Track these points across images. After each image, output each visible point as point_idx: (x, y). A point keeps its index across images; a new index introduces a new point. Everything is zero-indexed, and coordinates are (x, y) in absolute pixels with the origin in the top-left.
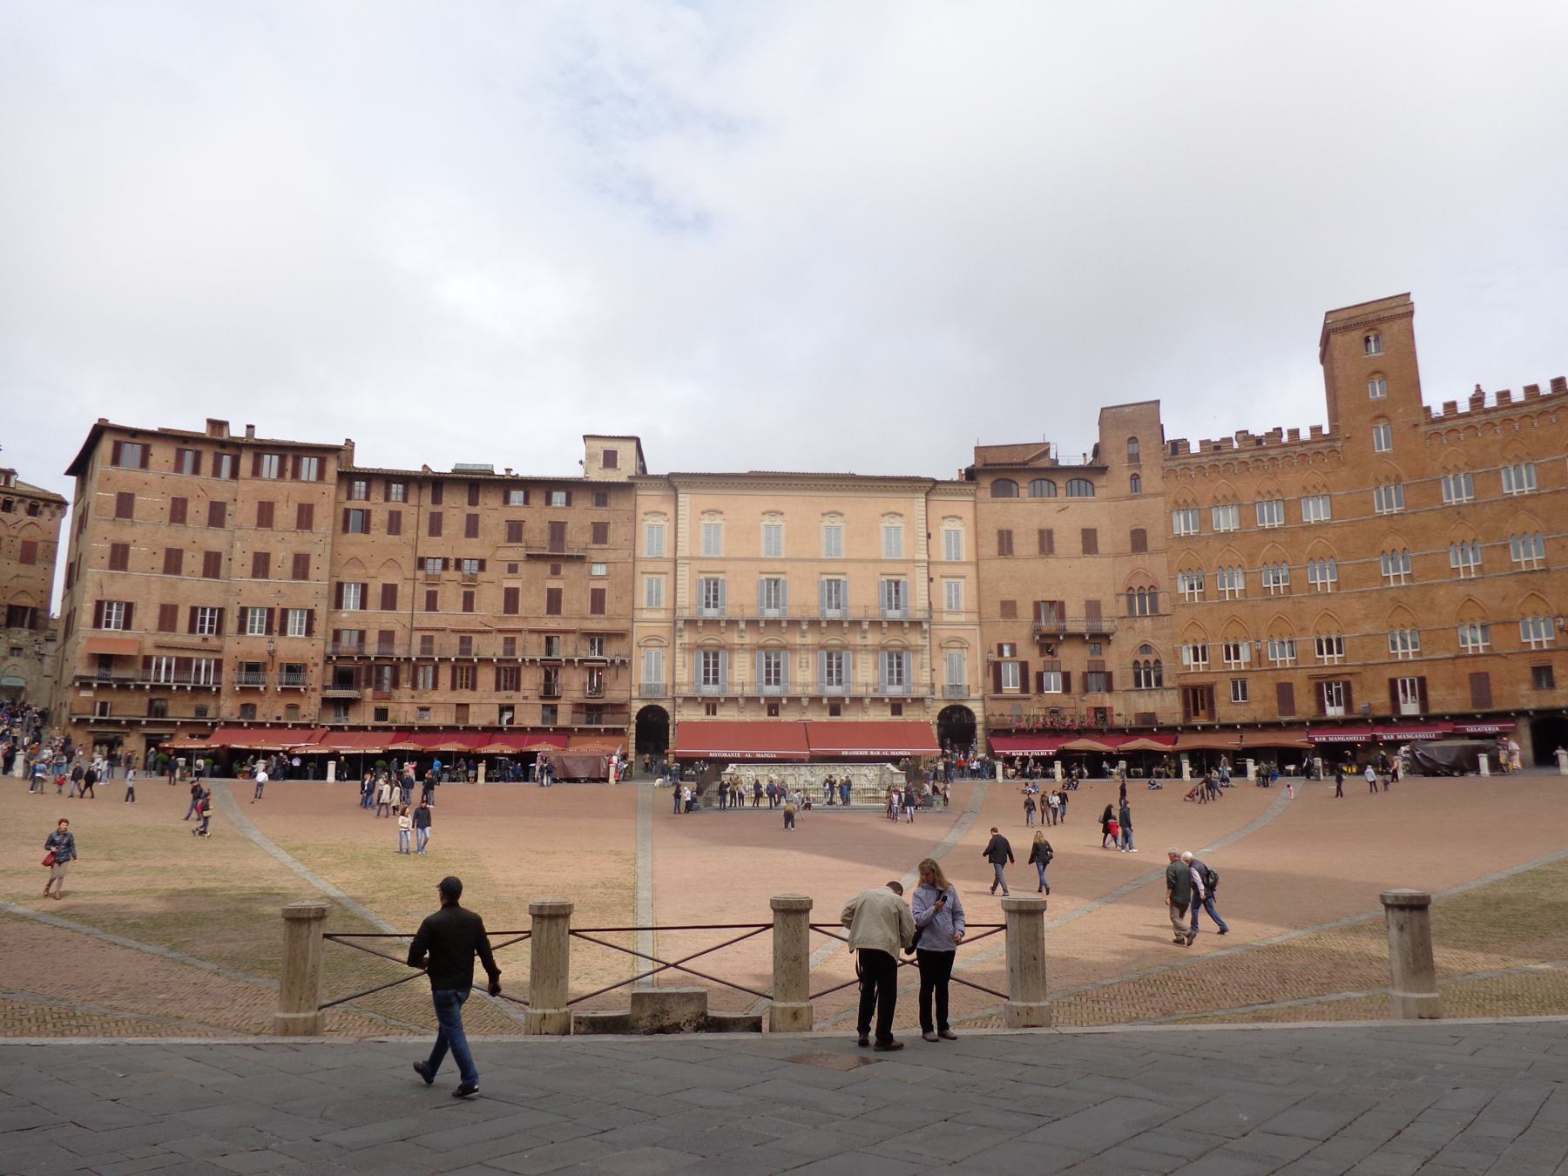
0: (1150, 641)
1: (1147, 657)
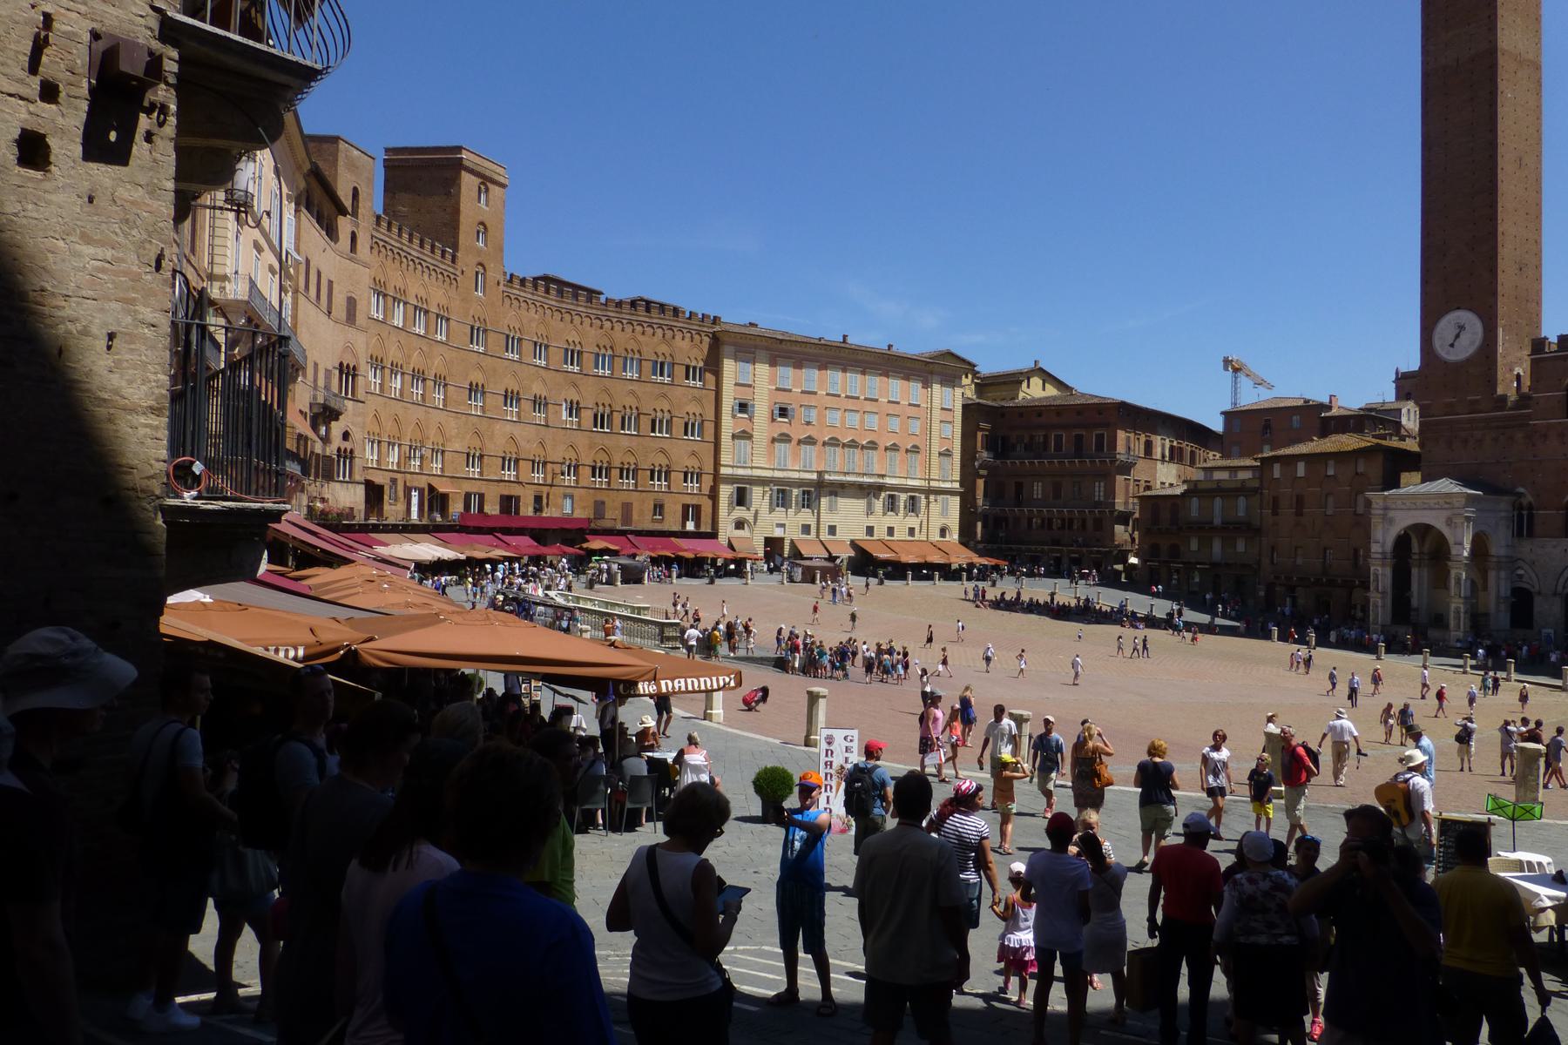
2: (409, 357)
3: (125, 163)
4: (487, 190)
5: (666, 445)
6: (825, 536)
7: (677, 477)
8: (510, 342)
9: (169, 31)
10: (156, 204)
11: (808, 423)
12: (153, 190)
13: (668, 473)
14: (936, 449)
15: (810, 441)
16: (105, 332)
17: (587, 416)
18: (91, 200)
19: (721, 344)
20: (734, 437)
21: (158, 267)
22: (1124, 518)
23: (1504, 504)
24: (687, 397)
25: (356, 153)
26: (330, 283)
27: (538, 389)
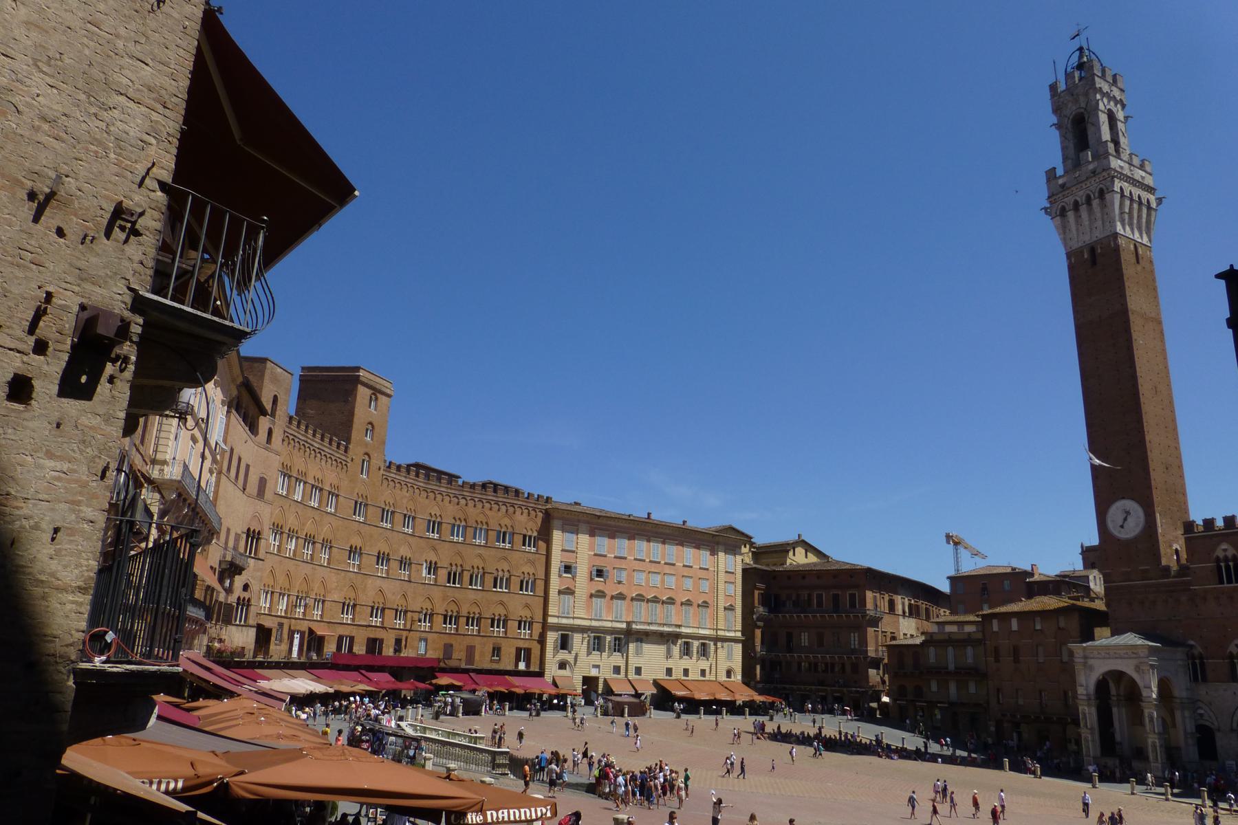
2: (304, 525)
3: (90, 398)
4: (376, 399)
5: (505, 598)
6: (632, 676)
7: (513, 625)
8: (384, 513)
9: (139, 305)
10: (109, 429)
11: (620, 582)
12: (108, 419)
13: (505, 622)
14: (722, 604)
15: (621, 597)
16: (51, 527)
17: (443, 574)
18: (58, 426)
19: (552, 518)
20: (560, 592)
21: (103, 476)
22: (876, 663)
23: (1180, 653)
24: (523, 560)
25: (279, 370)
26: (248, 466)
27: (404, 551)
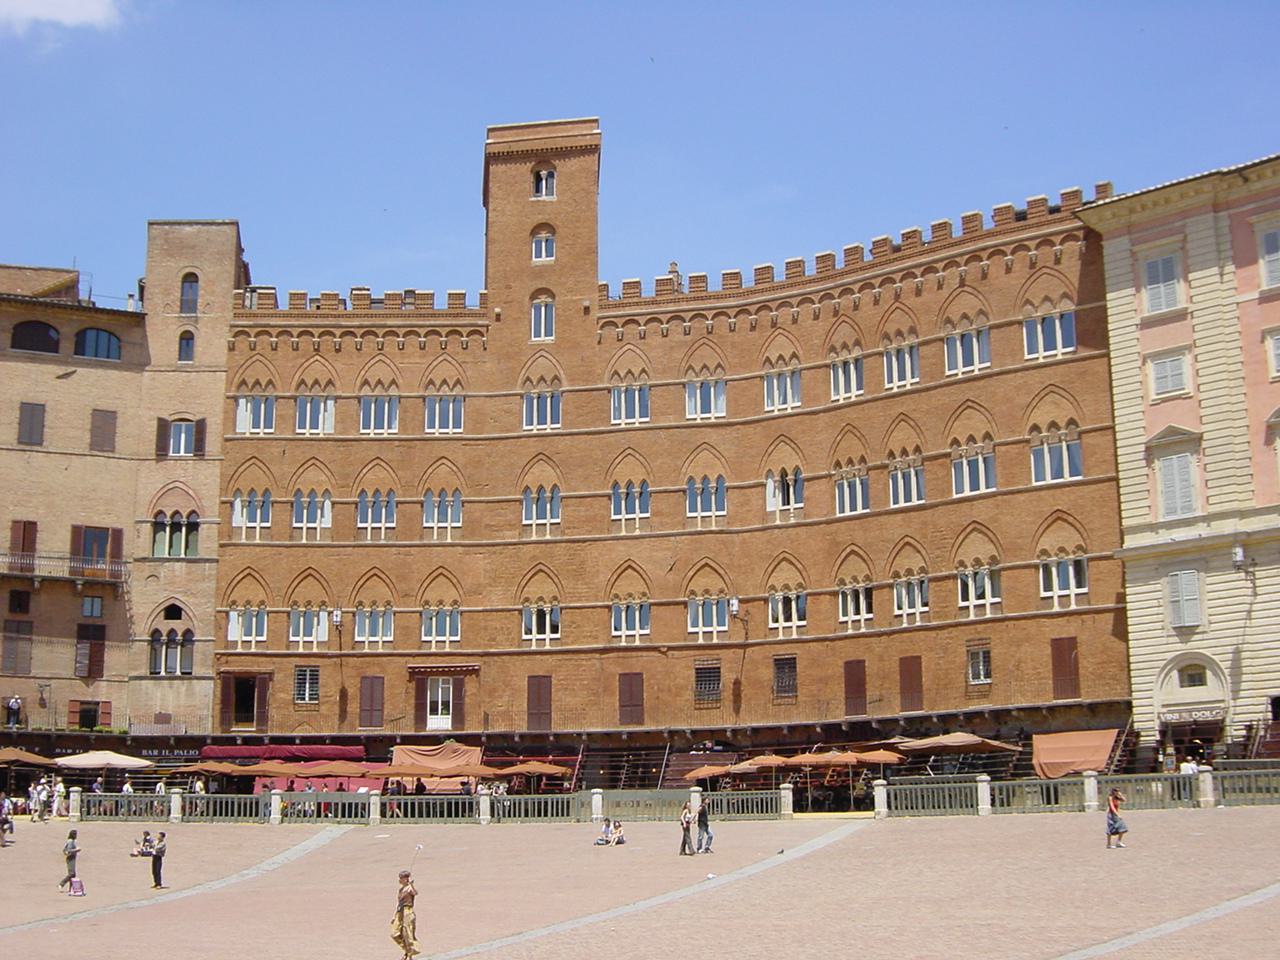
0: (182, 600)
1: (174, 624)
20: (1151, 452)
25: (188, 229)
